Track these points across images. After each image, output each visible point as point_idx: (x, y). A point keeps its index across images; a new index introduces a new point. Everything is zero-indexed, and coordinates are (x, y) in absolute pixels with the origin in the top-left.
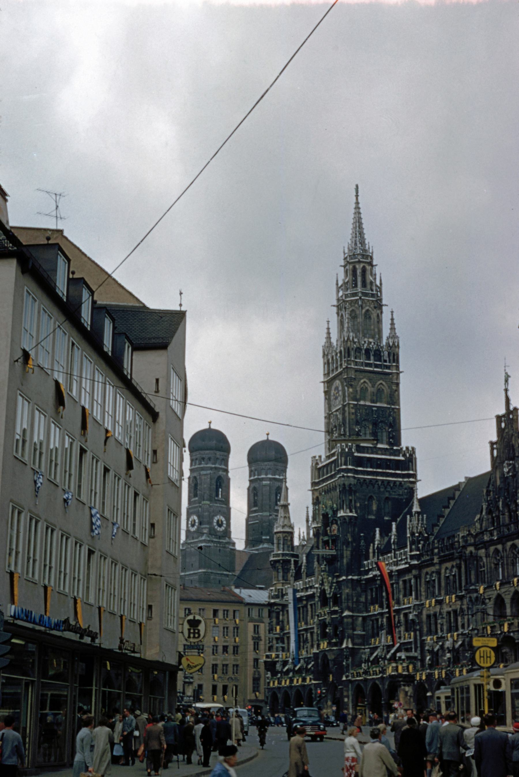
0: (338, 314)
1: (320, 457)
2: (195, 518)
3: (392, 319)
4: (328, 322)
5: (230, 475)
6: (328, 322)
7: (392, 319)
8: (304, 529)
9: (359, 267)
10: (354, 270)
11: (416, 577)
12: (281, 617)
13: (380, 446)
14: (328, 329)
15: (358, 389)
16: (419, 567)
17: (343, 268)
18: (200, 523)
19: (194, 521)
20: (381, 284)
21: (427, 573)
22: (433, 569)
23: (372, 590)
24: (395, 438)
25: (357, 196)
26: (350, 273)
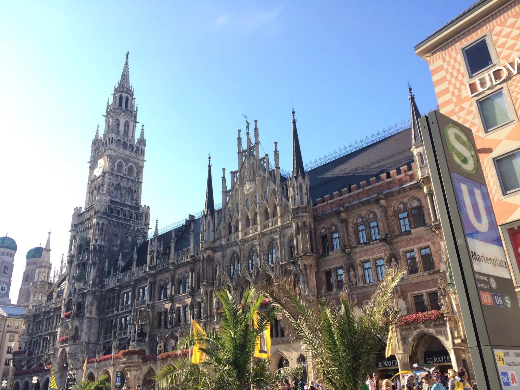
0: (106, 121)
3: (143, 129)
4: (98, 126)
5: (14, 263)
7: (143, 129)
8: (58, 269)
9: (124, 95)
10: (121, 98)
12: (31, 327)
13: (126, 203)
14: (98, 130)
15: (116, 164)
16: (154, 276)
22: (168, 275)
23: (110, 299)
24: (137, 200)
25: (127, 58)
26: (118, 98)
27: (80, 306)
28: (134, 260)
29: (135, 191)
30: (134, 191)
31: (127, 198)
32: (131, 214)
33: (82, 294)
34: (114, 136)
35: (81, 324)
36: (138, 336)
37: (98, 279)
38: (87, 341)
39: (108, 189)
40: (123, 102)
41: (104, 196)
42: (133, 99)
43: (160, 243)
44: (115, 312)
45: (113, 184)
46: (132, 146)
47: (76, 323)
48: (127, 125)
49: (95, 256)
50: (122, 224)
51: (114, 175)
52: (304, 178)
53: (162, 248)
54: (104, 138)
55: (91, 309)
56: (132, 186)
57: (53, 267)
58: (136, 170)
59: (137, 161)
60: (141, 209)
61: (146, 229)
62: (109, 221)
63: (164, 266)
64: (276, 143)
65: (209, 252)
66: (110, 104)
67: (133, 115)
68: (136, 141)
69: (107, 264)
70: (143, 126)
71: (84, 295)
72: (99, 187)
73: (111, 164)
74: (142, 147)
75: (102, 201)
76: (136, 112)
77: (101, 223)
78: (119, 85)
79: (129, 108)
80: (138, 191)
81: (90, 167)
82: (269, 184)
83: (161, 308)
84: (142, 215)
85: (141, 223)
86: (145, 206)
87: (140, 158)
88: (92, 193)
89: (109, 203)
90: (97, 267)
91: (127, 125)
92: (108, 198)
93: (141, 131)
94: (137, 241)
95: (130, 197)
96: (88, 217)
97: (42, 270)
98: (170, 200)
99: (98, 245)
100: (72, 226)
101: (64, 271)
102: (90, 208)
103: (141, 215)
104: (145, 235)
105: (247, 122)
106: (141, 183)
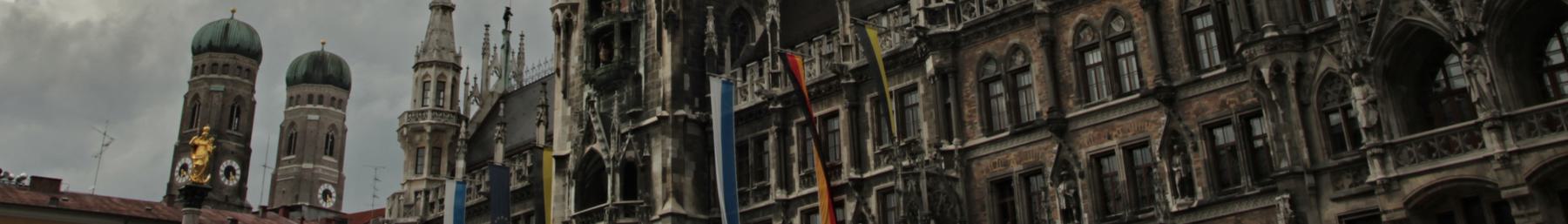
5: (256, 97)
27: (635, 176)
33: (633, 132)
37: (687, 77)
44: (778, 194)
55: (681, 185)
57: (463, 64)
69: (711, 25)
71: (642, 136)
83: (1006, 164)
90: (681, 32)
97: (432, 72)
101: (494, 79)
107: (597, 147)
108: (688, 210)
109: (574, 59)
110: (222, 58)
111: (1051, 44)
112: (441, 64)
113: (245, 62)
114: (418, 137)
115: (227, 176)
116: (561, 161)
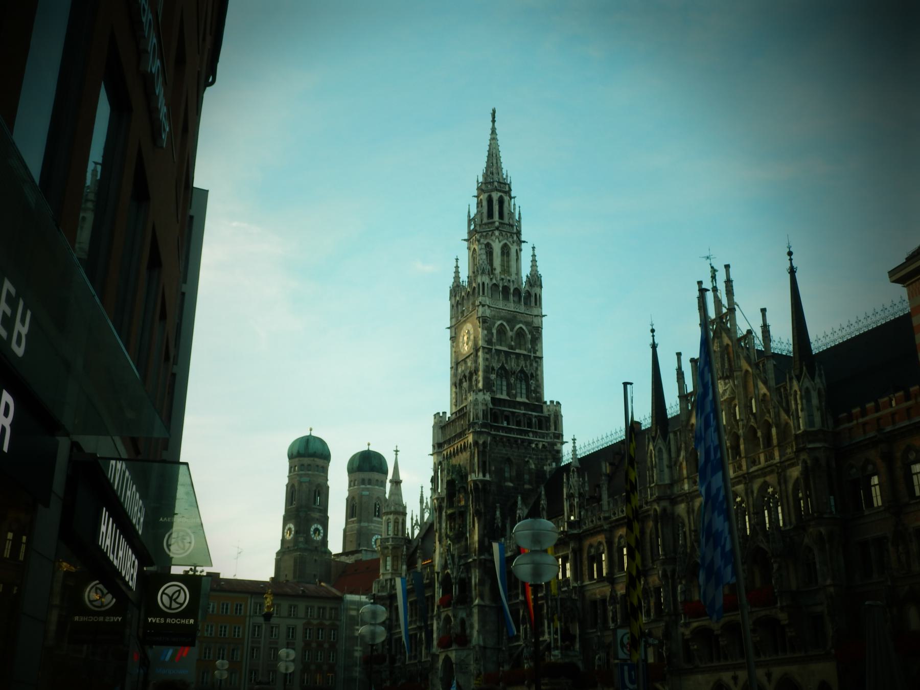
0: (469, 248)
1: (444, 413)
2: (292, 526)
3: (534, 256)
4: (457, 259)
5: (329, 483)
6: (457, 259)
7: (534, 256)
8: (417, 512)
9: (495, 196)
10: (490, 201)
11: (574, 551)
13: (518, 399)
14: (457, 267)
15: (494, 331)
16: (579, 538)
17: (476, 199)
18: (297, 532)
19: (290, 529)
20: (520, 218)
21: (591, 546)
22: (601, 538)
25: (494, 121)
26: (485, 203)
27: (464, 585)
28: (543, 508)
29: (532, 375)
30: (530, 376)
31: (519, 390)
32: (530, 419)
33: (463, 565)
34: (486, 279)
35: (470, 615)
36: (563, 640)
38: (482, 643)
39: (486, 380)
40: (495, 217)
41: (481, 393)
42: (511, 198)
43: (584, 479)
45: (493, 369)
46: (517, 292)
47: (462, 614)
48: (505, 251)
49: (477, 500)
50: (516, 440)
51: (494, 351)
52: (813, 379)
53: (587, 489)
54: (470, 283)
56: (526, 366)
57: (408, 511)
58: (529, 336)
59: (529, 319)
60: (545, 409)
61: (559, 445)
62: (494, 437)
63: (592, 521)
64: (763, 311)
65: (665, 504)
66: (472, 216)
67: (515, 231)
68: (524, 279)
69: (498, 513)
70: (534, 248)
71: (468, 567)
72: (471, 374)
73: (486, 332)
74: (537, 290)
75: (479, 399)
76: (519, 221)
77: (481, 442)
78: (485, 176)
79: (506, 220)
80: (537, 375)
81: (451, 338)
82: (756, 386)
84: (548, 419)
85: (548, 434)
86: (552, 402)
87: (535, 312)
88: (461, 386)
89: (491, 406)
91: (505, 251)
92: (488, 397)
93: (531, 259)
94: (545, 468)
95: (524, 386)
96: (458, 431)
97: (391, 517)
98: (593, 396)
99: (481, 481)
100: (434, 446)
101: (427, 515)
102: (460, 414)
103: (548, 421)
104: (557, 456)
105: (712, 267)
106: (541, 358)
107: (449, 571)
108: (487, 602)
109: (444, 525)
110: (306, 461)
111: (610, 543)
112: (396, 513)
113: (320, 462)
114: (386, 551)
115: (315, 533)
116: (438, 573)
